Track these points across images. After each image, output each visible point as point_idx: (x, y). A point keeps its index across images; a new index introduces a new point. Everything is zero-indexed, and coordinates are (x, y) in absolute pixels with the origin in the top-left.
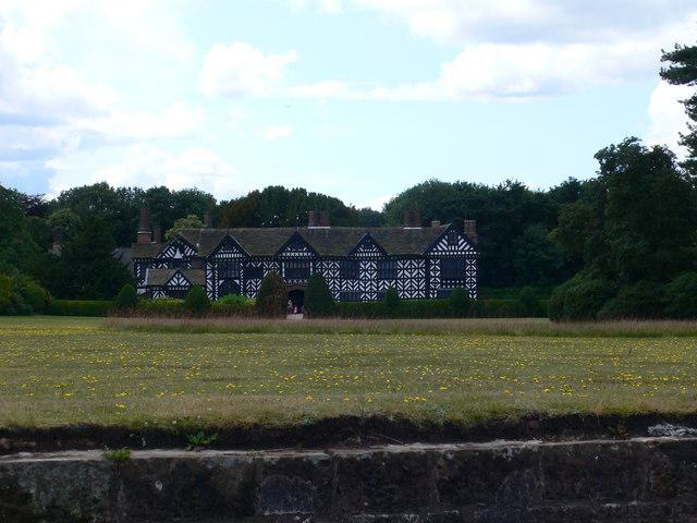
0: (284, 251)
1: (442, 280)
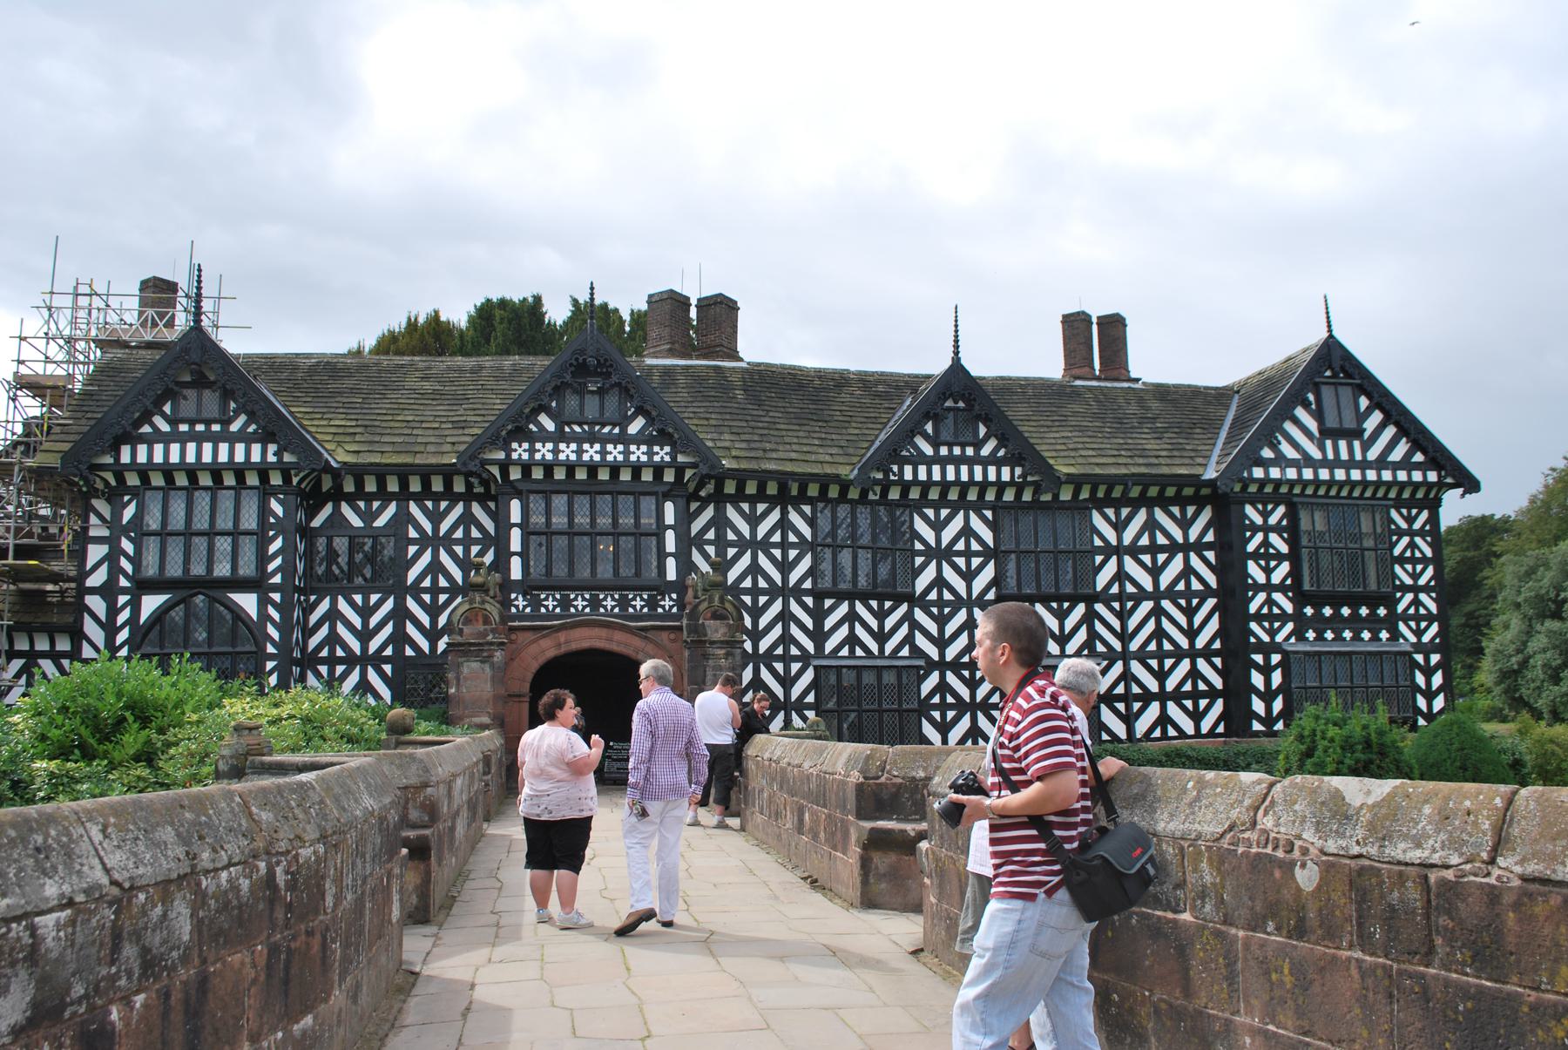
0: (520, 433)
1: (1300, 598)
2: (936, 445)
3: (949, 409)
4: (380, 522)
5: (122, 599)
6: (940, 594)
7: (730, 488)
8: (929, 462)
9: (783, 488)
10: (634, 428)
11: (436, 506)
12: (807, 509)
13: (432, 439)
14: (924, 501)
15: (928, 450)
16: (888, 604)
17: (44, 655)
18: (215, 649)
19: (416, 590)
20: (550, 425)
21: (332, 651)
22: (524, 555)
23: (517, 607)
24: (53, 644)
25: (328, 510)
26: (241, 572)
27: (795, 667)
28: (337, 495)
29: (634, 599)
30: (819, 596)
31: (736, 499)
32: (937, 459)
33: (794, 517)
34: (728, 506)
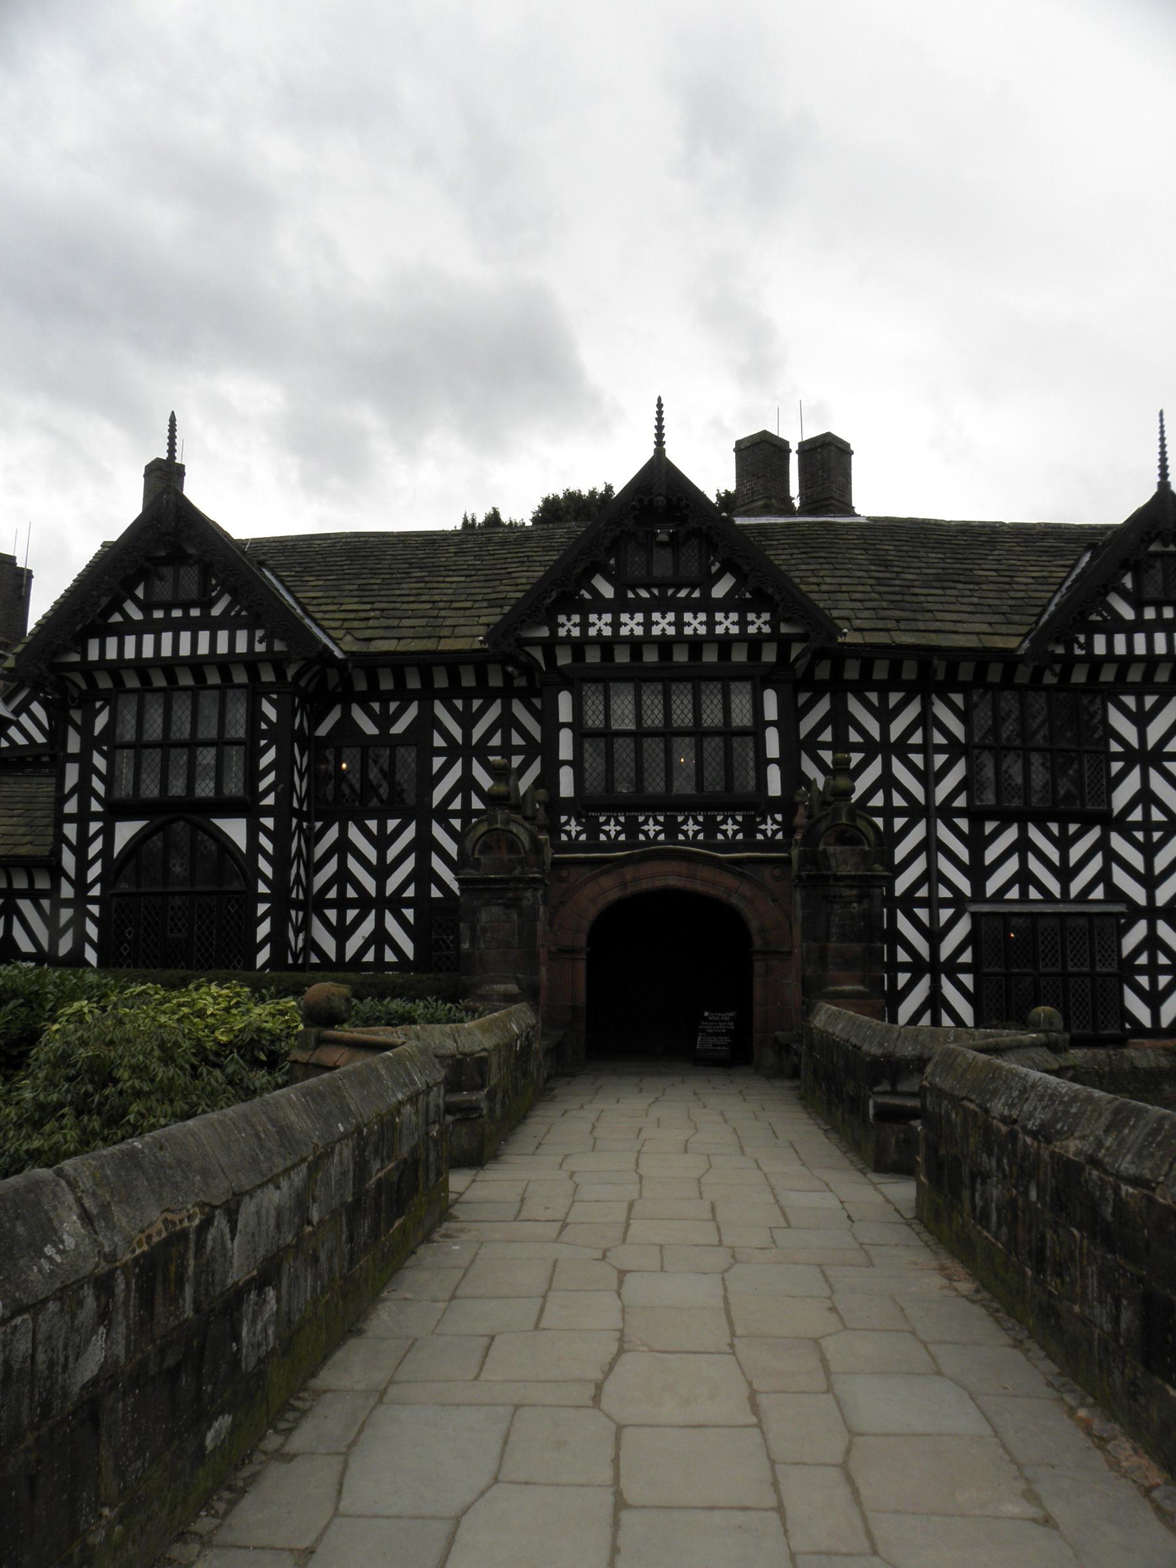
0: (571, 604)
2: (1138, 606)
3: (1156, 555)
4: (398, 728)
5: (94, 827)
6: (1147, 813)
7: (852, 671)
8: (1129, 629)
9: (925, 669)
10: (719, 591)
11: (467, 706)
12: (958, 699)
13: (462, 621)
14: (1121, 685)
15: (1128, 613)
16: (1073, 828)
17: (23, 894)
18: (199, 888)
19: (443, 814)
20: (608, 591)
21: (342, 892)
22: (577, 764)
23: (568, 833)
24: (31, 882)
25: (335, 715)
26: (226, 791)
27: (945, 914)
28: (347, 697)
29: (724, 822)
30: (976, 816)
31: (859, 689)
32: (1139, 625)
33: (941, 711)
34: (850, 696)
